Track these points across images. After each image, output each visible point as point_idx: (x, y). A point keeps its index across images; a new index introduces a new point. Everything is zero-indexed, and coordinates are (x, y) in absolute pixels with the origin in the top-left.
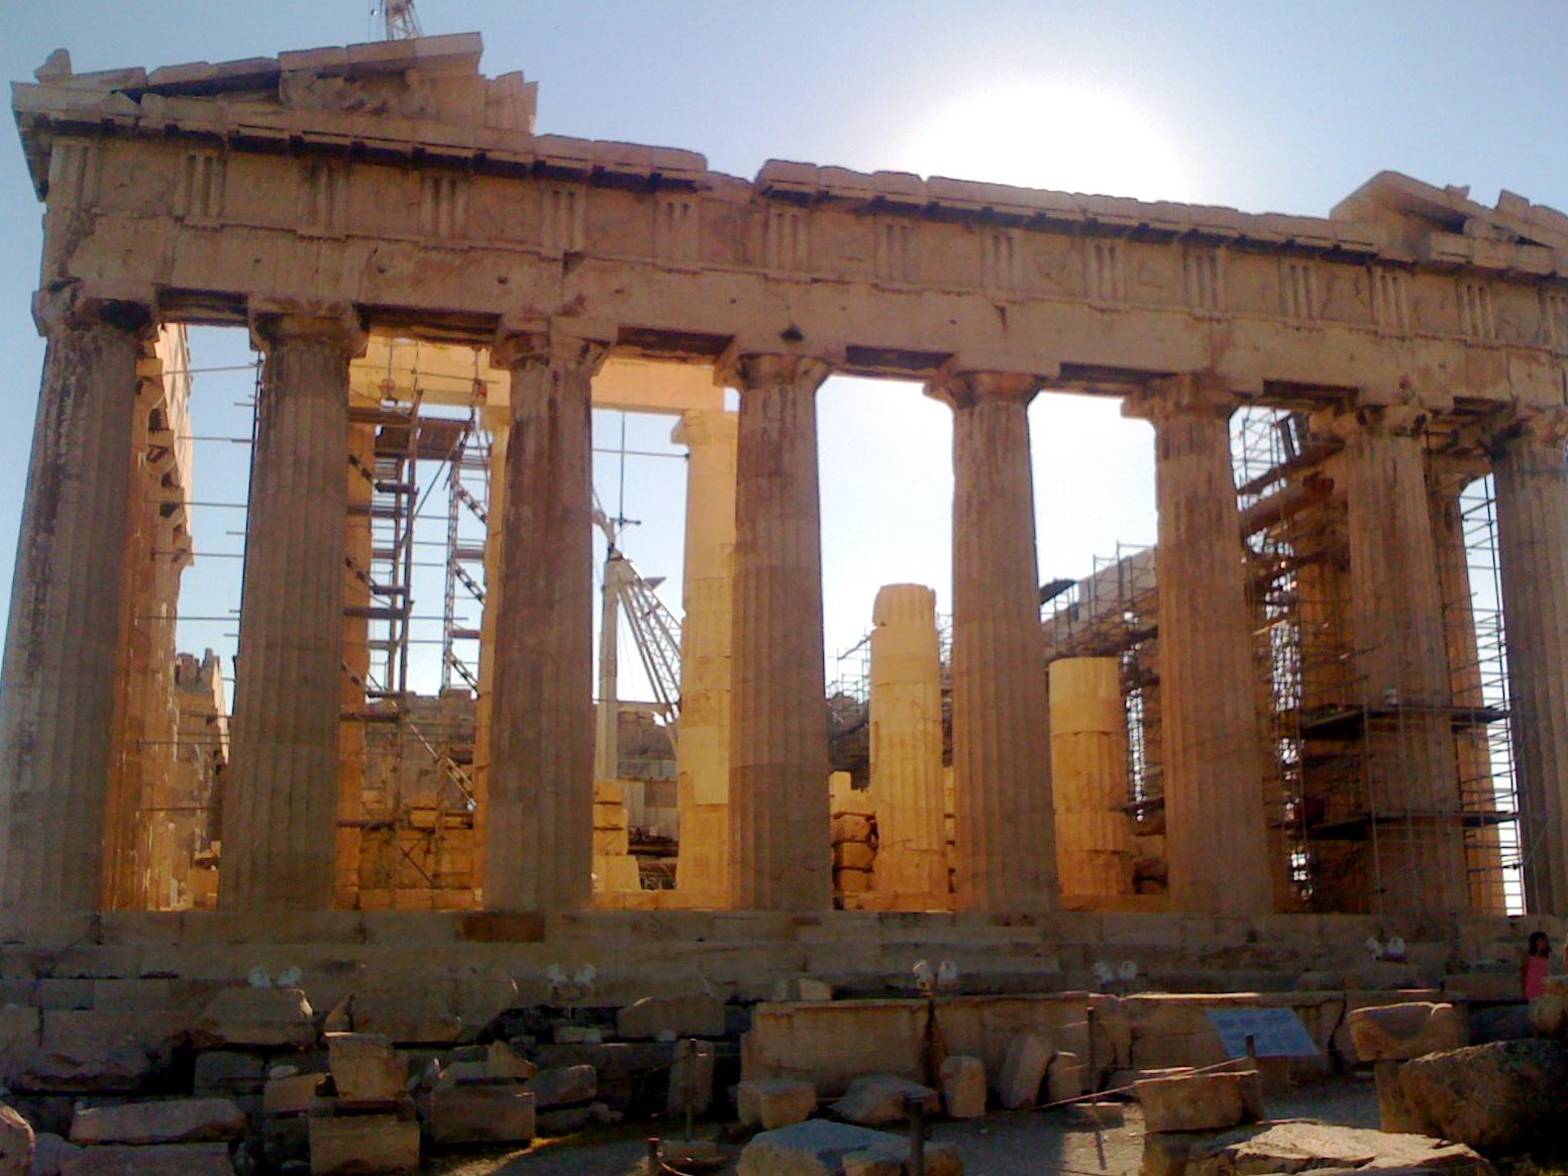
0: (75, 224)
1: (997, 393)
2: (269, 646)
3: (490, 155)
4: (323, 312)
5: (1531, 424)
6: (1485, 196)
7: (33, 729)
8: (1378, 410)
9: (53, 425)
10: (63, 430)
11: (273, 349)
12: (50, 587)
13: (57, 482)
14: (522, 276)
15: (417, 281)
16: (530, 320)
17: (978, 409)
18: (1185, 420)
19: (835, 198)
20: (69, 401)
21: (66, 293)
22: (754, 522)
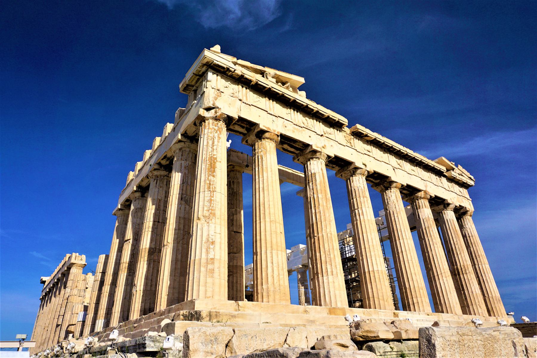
0: (216, 93)
8: (449, 204)
10: (215, 147)
12: (215, 193)
16: (318, 147)
17: (392, 191)
19: (369, 136)
21: (213, 111)
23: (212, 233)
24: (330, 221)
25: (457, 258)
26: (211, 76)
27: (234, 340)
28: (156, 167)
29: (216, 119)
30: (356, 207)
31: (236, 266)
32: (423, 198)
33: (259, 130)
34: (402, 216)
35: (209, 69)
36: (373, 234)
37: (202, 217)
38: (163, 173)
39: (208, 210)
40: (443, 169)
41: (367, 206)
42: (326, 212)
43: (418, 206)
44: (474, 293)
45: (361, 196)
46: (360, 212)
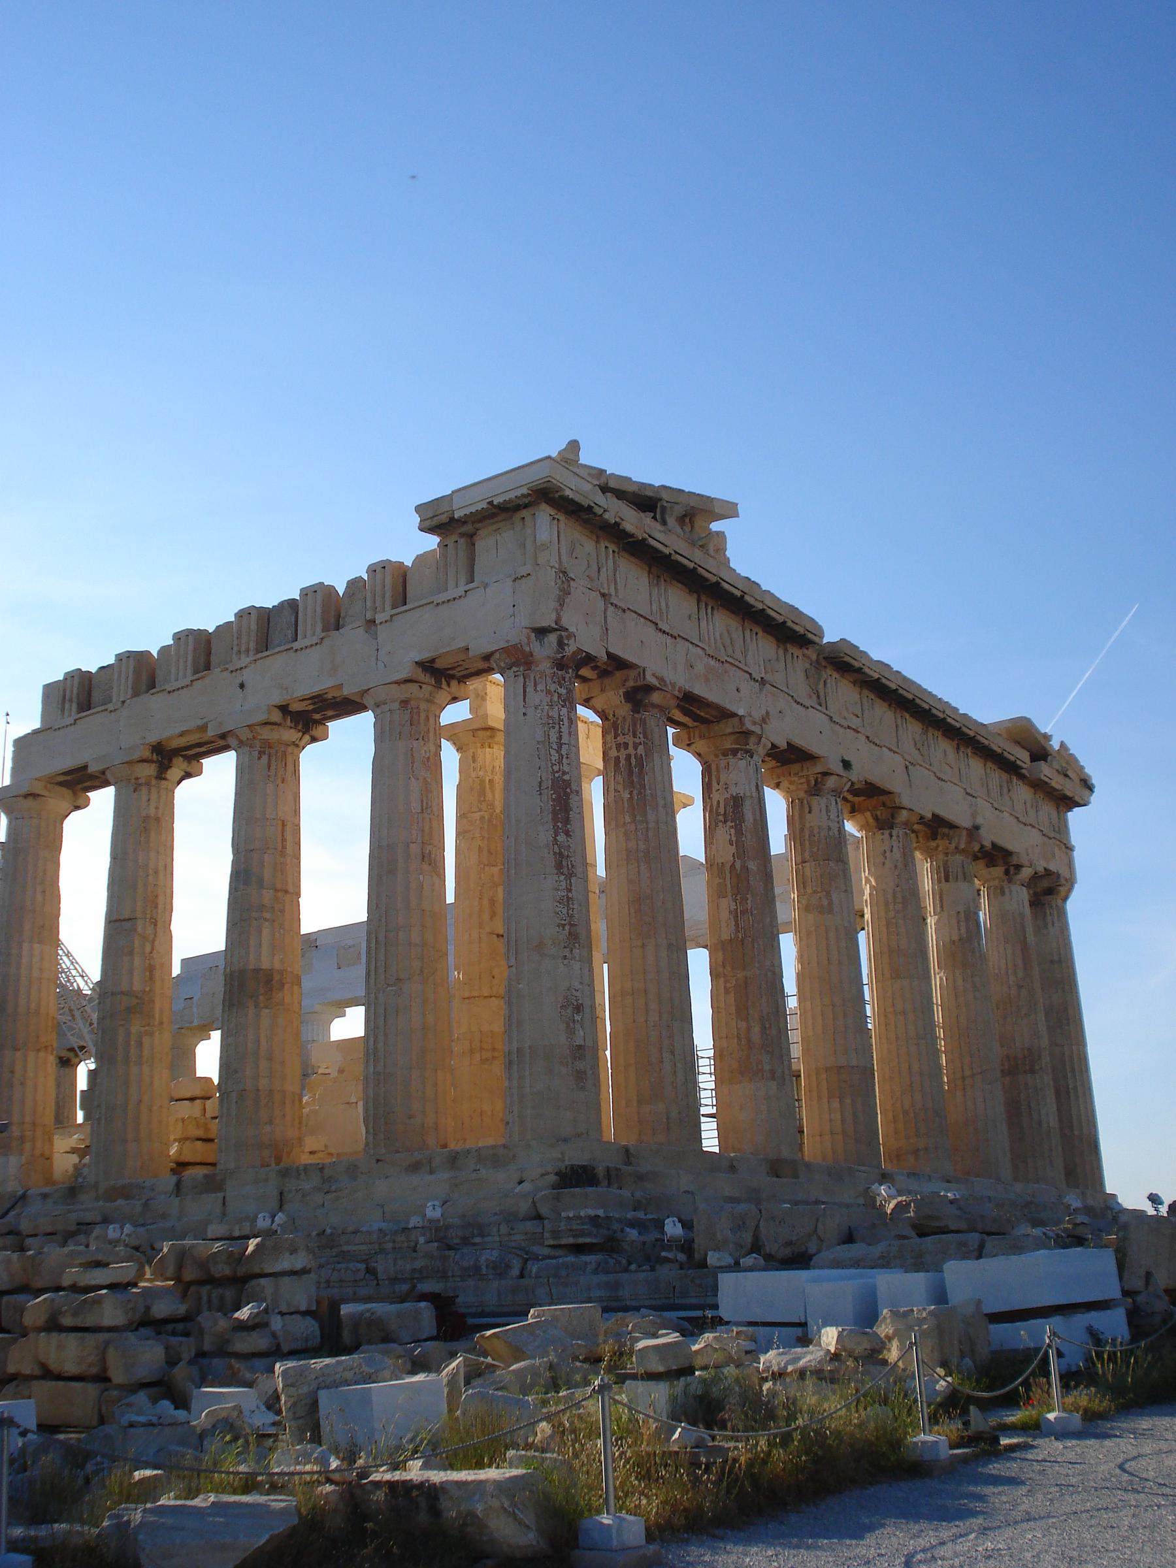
1: (906, 824)
2: (669, 946)
3: (747, 598)
4: (676, 693)
5: (1061, 888)
6: (1055, 744)
7: (578, 994)
9: (555, 746)
10: (564, 752)
11: (636, 710)
12: (573, 880)
13: (567, 795)
14: (748, 688)
15: (707, 680)
16: (755, 723)
17: (894, 833)
18: (959, 858)
19: (864, 673)
20: (565, 729)
21: (552, 638)
22: (828, 894)
26: (544, 524)
27: (762, 1224)
28: (276, 716)
29: (560, 665)
33: (639, 683)
35: (544, 506)
38: (291, 735)
39: (564, 926)
40: (1022, 756)
44: (1045, 1125)
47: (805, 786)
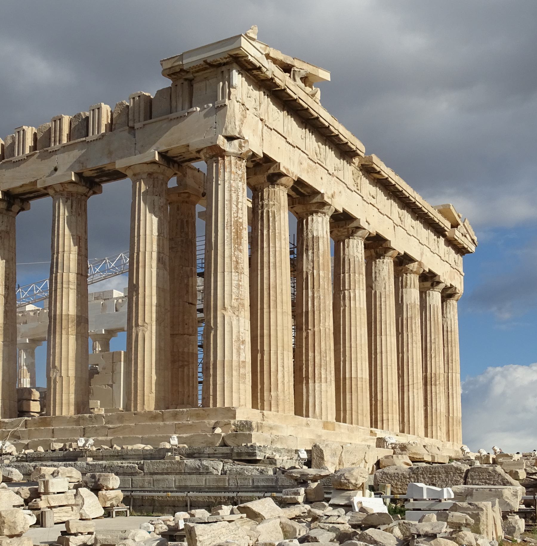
15: (308, 172)
16: (329, 198)
17: (385, 261)
23: (242, 330)
24: (330, 312)
25: (428, 363)
29: (240, 157)
30: (347, 288)
31: (193, 353)
32: (415, 273)
33: (276, 171)
34: (391, 302)
36: (363, 329)
37: (229, 308)
41: (361, 287)
42: (327, 298)
43: (404, 284)
45: (356, 272)
46: (352, 295)
47: (346, 233)
